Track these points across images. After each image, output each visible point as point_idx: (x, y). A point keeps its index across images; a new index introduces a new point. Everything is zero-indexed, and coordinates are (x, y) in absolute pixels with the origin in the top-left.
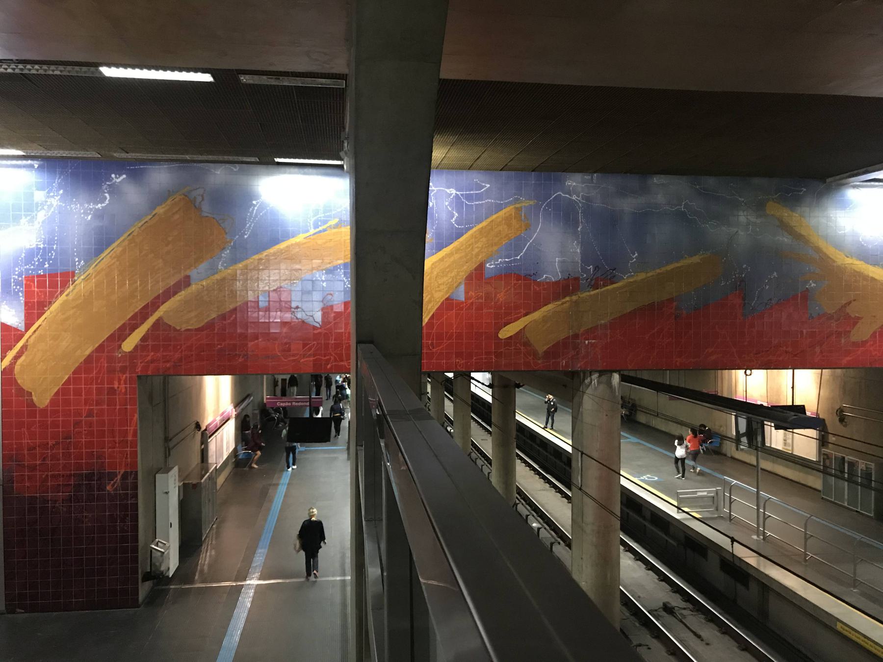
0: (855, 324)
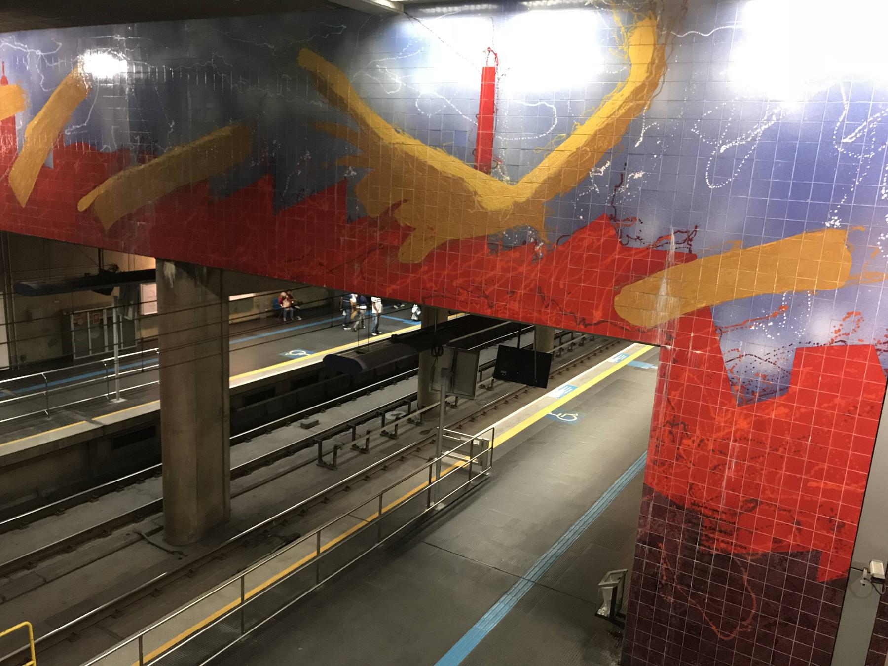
0: (405, 236)
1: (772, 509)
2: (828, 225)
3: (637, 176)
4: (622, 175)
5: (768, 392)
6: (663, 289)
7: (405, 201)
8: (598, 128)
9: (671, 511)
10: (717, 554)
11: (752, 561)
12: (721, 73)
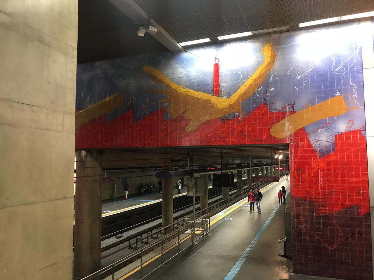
1: (339, 193)
2: (336, 95)
3: (272, 90)
4: (267, 90)
5: (328, 152)
6: (287, 124)
7: (187, 110)
8: (256, 77)
9: (302, 203)
10: (322, 215)
11: (335, 214)
12: (294, 56)
